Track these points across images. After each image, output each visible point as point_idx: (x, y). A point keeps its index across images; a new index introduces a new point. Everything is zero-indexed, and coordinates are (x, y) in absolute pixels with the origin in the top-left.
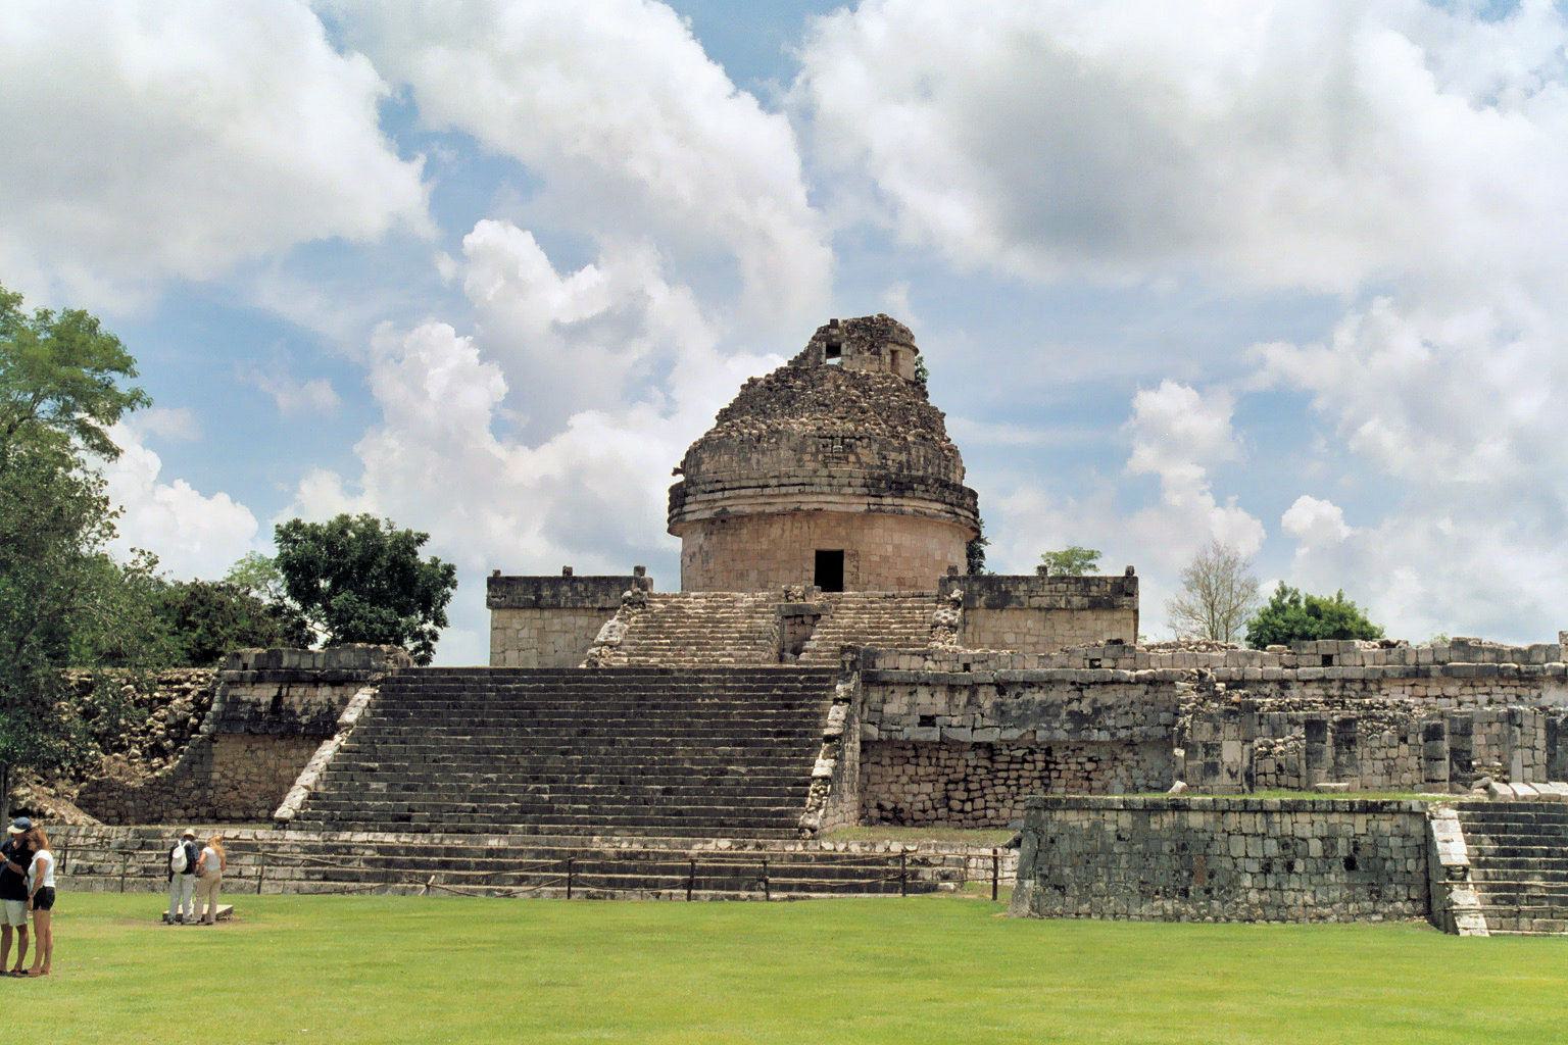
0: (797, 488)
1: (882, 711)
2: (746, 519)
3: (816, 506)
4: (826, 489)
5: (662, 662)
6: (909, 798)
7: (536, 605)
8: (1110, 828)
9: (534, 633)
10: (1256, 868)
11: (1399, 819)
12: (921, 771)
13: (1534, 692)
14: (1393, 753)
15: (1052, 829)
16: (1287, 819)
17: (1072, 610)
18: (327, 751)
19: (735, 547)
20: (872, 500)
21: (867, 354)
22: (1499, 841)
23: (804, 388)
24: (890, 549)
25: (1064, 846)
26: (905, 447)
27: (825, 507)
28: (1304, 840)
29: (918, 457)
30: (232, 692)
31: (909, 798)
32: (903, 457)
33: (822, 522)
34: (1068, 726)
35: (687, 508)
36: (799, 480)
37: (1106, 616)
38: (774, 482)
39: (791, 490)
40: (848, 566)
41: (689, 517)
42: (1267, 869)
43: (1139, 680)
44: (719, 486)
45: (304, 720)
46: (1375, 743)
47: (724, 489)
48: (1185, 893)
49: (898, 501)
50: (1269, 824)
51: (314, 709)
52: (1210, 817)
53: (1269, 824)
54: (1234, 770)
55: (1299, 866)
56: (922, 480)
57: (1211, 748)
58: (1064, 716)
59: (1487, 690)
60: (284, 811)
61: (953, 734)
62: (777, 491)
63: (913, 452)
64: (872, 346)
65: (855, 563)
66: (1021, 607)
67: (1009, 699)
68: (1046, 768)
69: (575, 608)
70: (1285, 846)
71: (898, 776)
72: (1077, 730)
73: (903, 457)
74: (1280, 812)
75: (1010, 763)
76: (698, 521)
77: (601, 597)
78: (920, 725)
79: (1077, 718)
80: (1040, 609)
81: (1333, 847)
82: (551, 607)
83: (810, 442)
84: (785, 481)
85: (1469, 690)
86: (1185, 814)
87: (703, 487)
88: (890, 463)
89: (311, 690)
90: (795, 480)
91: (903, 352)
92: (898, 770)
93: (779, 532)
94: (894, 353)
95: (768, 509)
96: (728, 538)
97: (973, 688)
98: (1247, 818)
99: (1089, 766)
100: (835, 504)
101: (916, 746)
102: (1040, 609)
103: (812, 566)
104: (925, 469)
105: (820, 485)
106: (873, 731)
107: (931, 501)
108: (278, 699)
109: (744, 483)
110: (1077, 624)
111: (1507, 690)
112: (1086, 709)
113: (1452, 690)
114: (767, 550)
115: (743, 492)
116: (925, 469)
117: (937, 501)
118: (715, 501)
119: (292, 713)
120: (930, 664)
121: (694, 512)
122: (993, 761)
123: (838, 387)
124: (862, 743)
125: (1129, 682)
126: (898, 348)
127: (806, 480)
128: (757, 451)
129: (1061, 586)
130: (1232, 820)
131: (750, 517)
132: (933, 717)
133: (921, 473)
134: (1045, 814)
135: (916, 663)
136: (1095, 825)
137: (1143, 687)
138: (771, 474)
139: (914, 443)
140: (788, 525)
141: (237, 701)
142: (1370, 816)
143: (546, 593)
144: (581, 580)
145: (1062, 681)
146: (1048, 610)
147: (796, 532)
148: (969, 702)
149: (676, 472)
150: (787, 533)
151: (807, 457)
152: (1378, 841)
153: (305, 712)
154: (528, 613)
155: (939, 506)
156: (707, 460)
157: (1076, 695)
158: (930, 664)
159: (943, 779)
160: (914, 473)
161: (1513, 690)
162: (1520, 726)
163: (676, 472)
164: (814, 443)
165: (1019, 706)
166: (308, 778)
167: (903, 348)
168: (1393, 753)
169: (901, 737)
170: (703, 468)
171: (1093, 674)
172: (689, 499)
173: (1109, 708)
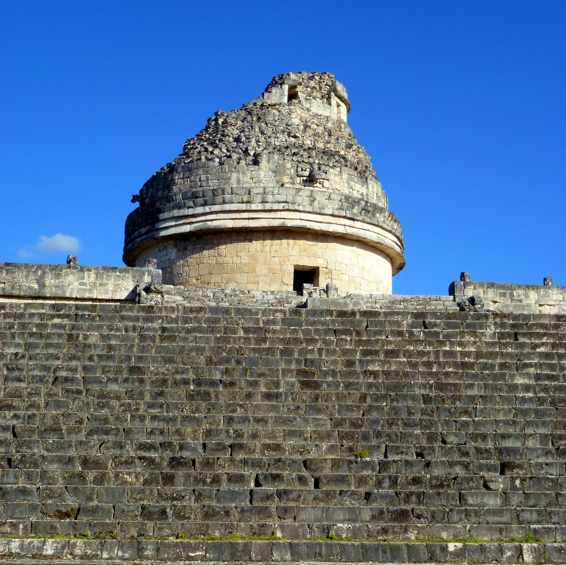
2: (223, 235)
27: (309, 225)
32: (364, 190)
38: (259, 198)
41: (163, 233)
47: (205, 204)
63: (370, 186)
73: (364, 190)
83: (289, 165)
88: (355, 193)
107: (387, 230)
114: (246, 265)
117: (390, 232)
118: (194, 216)
127: (290, 199)
143: (50, 281)
163: (135, 199)
172: (162, 216)
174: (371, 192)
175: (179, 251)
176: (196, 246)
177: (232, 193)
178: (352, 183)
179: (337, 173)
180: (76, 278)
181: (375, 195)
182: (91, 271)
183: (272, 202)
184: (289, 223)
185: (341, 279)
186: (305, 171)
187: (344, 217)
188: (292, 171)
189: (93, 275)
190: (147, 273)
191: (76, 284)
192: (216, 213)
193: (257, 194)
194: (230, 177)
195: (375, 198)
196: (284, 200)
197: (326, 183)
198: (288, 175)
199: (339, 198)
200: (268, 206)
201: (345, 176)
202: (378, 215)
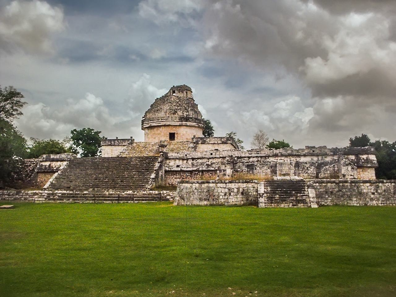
0: (165, 120)
5: (133, 156)
7: (111, 145)
8: (194, 187)
9: (110, 150)
10: (223, 194)
11: (253, 184)
12: (177, 177)
13: (299, 158)
14: (267, 171)
15: (182, 187)
16: (230, 184)
17: (218, 144)
18: (56, 175)
21: (181, 93)
22: (271, 188)
25: (184, 191)
26: (188, 112)
28: (233, 189)
30: (41, 163)
31: (175, 182)
32: (188, 113)
33: (170, 127)
34: (206, 167)
35: (144, 125)
37: (225, 145)
38: (160, 119)
40: (176, 136)
41: (144, 127)
42: (225, 195)
43: (220, 157)
45: (55, 169)
46: (263, 169)
47: (151, 121)
48: (209, 200)
49: (186, 122)
50: (226, 186)
51: (57, 166)
52: (214, 184)
53: (226, 186)
54: (229, 175)
55: (232, 194)
56: (191, 118)
57: (224, 170)
58: (205, 165)
59: (290, 158)
60: (45, 187)
61: (183, 169)
66: (208, 144)
67: (194, 162)
68: (202, 176)
69: (118, 145)
70: (229, 190)
72: (208, 167)
73: (188, 113)
74: (228, 183)
75: (195, 174)
76: (146, 127)
77: (124, 143)
78: (177, 167)
79: (208, 165)
80: (212, 144)
81: (239, 190)
82: (113, 145)
84: (163, 119)
85: (286, 158)
86: (209, 184)
89: (56, 163)
90: (165, 119)
91: (189, 92)
92: (173, 176)
94: (186, 92)
95: (159, 125)
97: (187, 159)
98: (222, 184)
99: (211, 175)
100: (173, 123)
101: (176, 171)
102: (212, 144)
103: (168, 136)
104: (192, 116)
106: (167, 169)
108: (50, 165)
109: (155, 119)
110: (219, 147)
111: (294, 158)
112: (209, 163)
113: (283, 158)
116: (192, 116)
119: (53, 167)
120: (179, 155)
122: (191, 174)
124: (165, 171)
125: (218, 158)
127: (167, 119)
129: (216, 139)
130: (219, 185)
132: (179, 166)
133: (191, 117)
134: (181, 184)
136: (191, 187)
137: (221, 159)
140: (163, 127)
141: (42, 165)
142: (247, 184)
143: (113, 142)
145: (205, 158)
146: (214, 144)
148: (187, 162)
149: (143, 117)
150: (163, 129)
151: (167, 114)
152: (248, 187)
153: (55, 167)
154: (109, 147)
155: (196, 123)
157: (208, 160)
158: (179, 155)
159: (181, 178)
160: (190, 117)
161: (295, 158)
162: (292, 165)
165: (196, 163)
166: (51, 180)
167: (189, 92)
168: (267, 171)
169: (173, 170)
170: (147, 116)
171: (211, 156)
172: (144, 123)
173: (214, 163)
184: (166, 124)
197: (177, 114)
200: (162, 121)
201: (181, 111)
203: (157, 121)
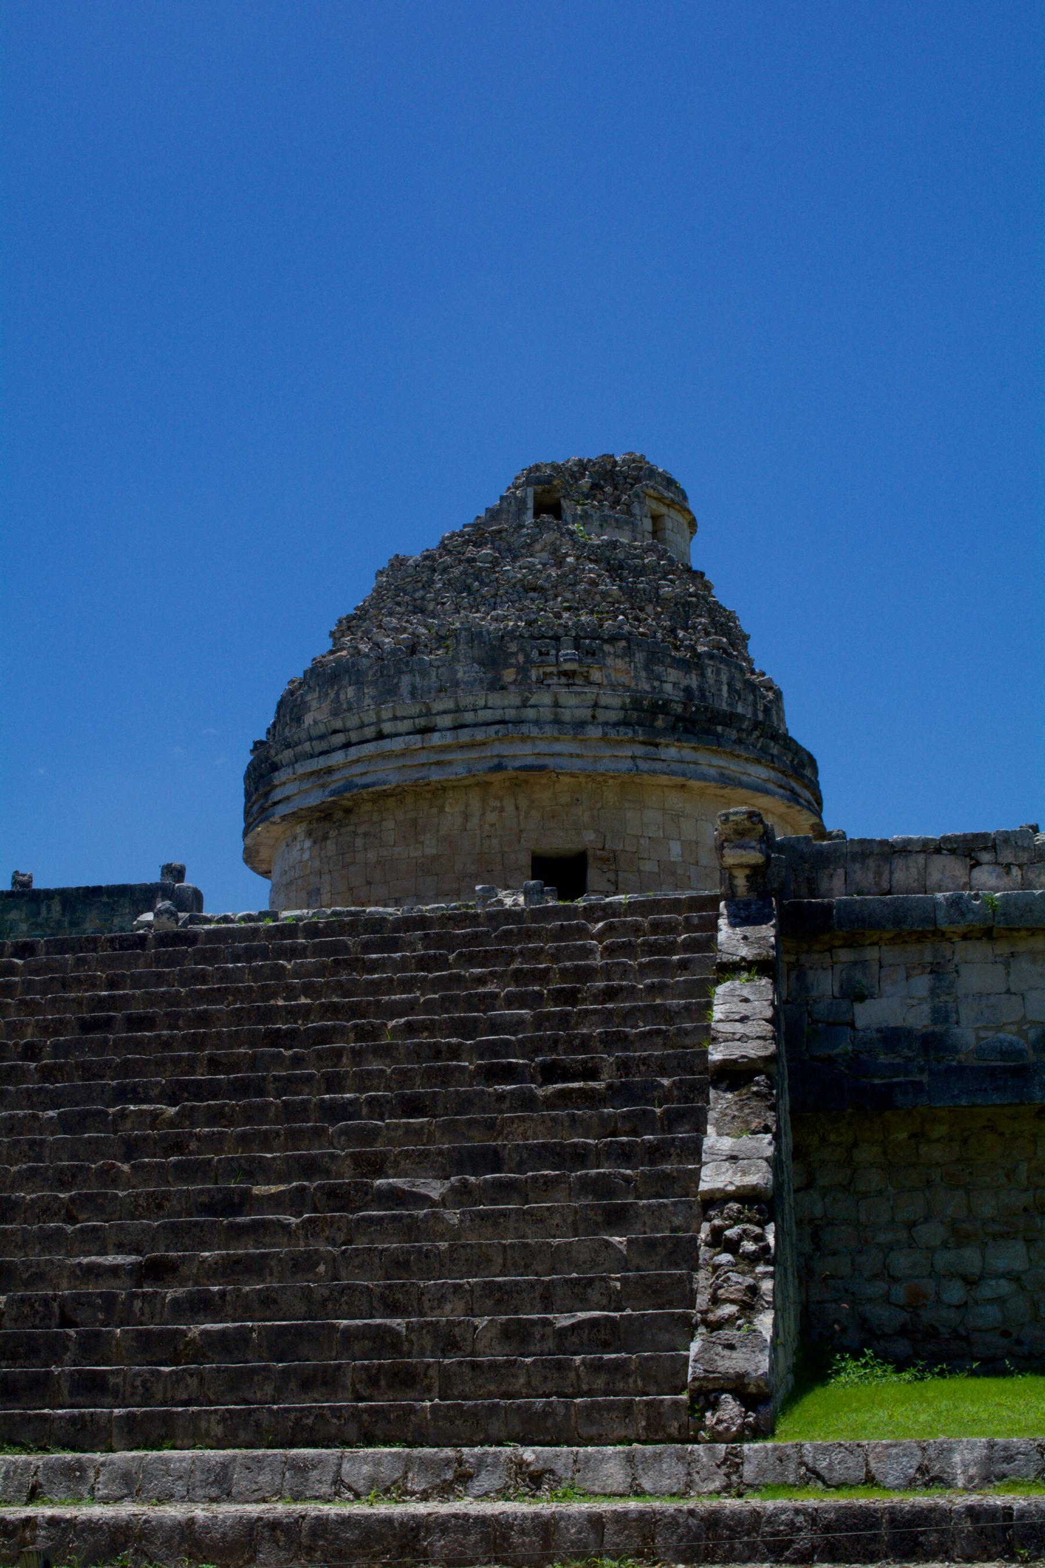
1: (852, 1025)
2: (391, 802)
3: (530, 761)
4: (550, 730)
6: (955, 1293)
19: (372, 856)
20: (640, 750)
23: (495, 562)
24: (676, 848)
29: (718, 682)
32: (693, 681)
35: (277, 795)
36: (498, 715)
38: (446, 721)
39: (480, 735)
44: (339, 739)
47: (348, 745)
49: (688, 754)
56: (731, 719)
62: (449, 738)
64: (617, 502)
65: (611, 875)
71: (911, 1225)
73: (693, 681)
84: (469, 717)
87: (307, 747)
88: (668, 687)
93: (459, 820)
94: (656, 519)
95: (436, 776)
96: (359, 842)
105: (537, 722)
109: (387, 727)
115: (387, 745)
117: (758, 761)
118: (330, 771)
121: (288, 798)
123: (560, 563)
126: (663, 510)
127: (510, 714)
128: (412, 671)
131: (397, 794)
135: (947, 871)
138: (438, 706)
139: (711, 656)
140: (475, 804)
144: (48, 895)
147: (492, 817)
150: (475, 821)
151: (509, 675)
156: (314, 704)
158: (985, 877)
164: (522, 649)
167: (673, 513)
172: (280, 777)
174: (711, 682)
175: (315, 842)
176: (343, 830)
177: (395, 718)
178: (658, 669)
179: (619, 652)
180: (23, 916)
181: (725, 688)
182: (52, 898)
183: (476, 725)
185: (639, 871)
186: (548, 654)
187: (632, 741)
188: (521, 658)
189: (56, 907)
190: (160, 893)
191: (24, 927)
192: (370, 758)
193: (445, 712)
194: (397, 684)
195: (725, 694)
196: (498, 718)
198: (512, 665)
199: (616, 702)
201: (640, 657)
202: (719, 729)
203: (416, 741)
